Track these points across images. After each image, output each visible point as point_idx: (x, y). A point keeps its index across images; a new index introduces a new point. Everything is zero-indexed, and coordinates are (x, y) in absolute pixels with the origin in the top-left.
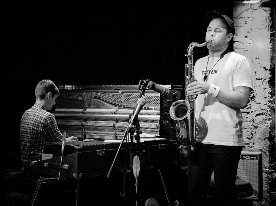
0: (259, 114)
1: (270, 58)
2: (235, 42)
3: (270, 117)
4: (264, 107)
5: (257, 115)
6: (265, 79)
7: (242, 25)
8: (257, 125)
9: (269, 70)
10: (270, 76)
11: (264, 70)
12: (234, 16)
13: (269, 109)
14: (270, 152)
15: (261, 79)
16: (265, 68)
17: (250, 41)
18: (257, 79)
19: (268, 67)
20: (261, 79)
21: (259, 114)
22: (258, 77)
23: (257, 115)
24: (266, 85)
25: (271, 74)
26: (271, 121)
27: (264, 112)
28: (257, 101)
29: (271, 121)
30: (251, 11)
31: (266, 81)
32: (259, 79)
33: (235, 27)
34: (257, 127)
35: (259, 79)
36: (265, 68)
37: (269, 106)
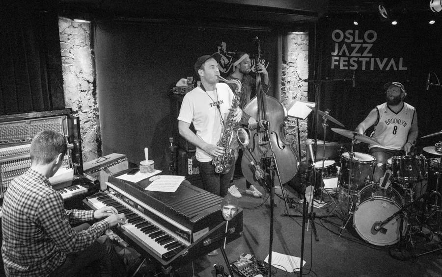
0: (87, 122)
1: (92, 72)
2: (62, 57)
3: (95, 123)
4: (90, 115)
5: (85, 122)
6: (89, 91)
7: (66, 41)
8: (86, 131)
9: (92, 83)
10: (93, 88)
11: (87, 83)
12: (60, 31)
13: (95, 116)
14: (97, 151)
15: (86, 91)
16: (88, 82)
17: (73, 57)
18: (81, 91)
19: (91, 80)
20: (86, 91)
21: (87, 122)
22: (82, 89)
23: (85, 122)
24: (90, 96)
25: (93, 86)
26: (96, 126)
27: (91, 119)
28: (84, 111)
29: (96, 126)
30: (72, 28)
31: (90, 92)
32: (84, 91)
33: (61, 43)
34: (86, 133)
35: (84, 91)
36: (88, 82)
37: (94, 114)
